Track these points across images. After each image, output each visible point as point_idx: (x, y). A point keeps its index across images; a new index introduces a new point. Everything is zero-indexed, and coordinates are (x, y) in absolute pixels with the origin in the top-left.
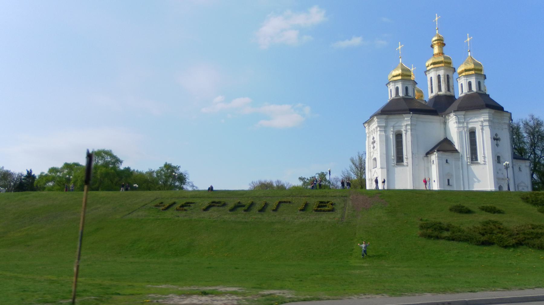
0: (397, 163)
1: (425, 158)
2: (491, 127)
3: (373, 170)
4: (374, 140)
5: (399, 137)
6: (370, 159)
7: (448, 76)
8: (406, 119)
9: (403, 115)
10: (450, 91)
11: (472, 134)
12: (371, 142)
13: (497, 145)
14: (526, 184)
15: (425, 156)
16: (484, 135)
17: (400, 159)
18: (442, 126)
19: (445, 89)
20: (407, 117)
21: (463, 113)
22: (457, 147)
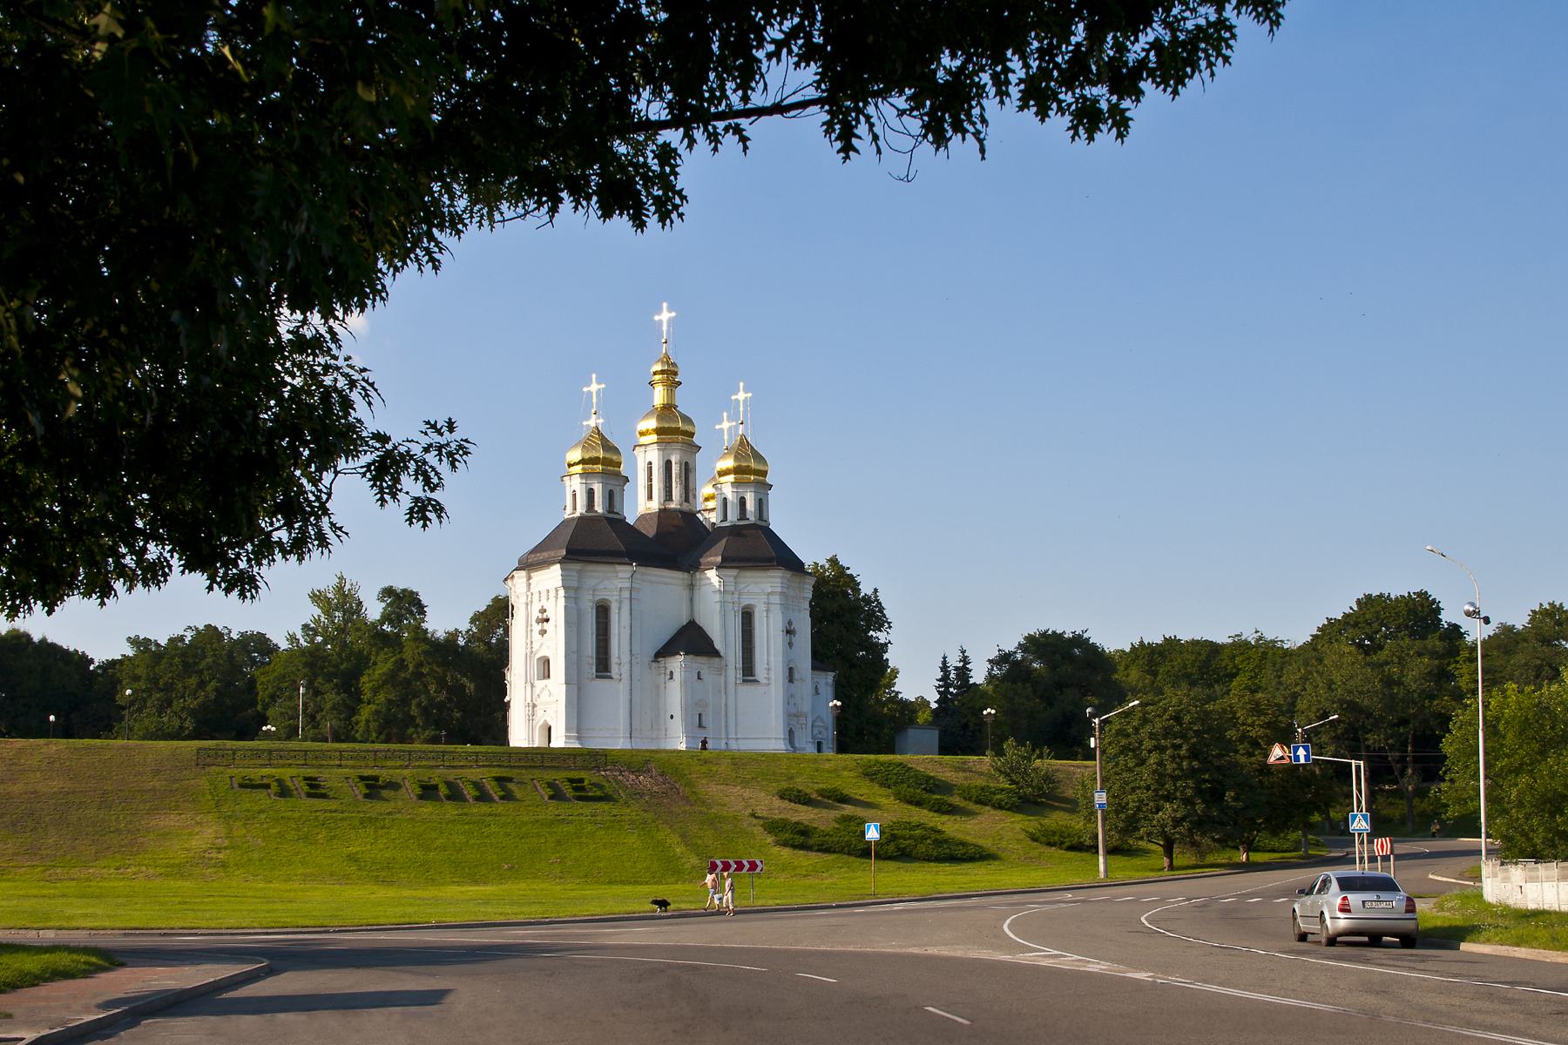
0: (598, 674)
1: (654, 665)
2: (785, 607)
3: (540, 684)
4: (545, 614)
5: (603, 611)
6: (530, 657)
7: (686, 463)
8: (620, 575)
9: (617, 566)
10: (689, 502)
11: (747, 617)
12: (534, 618)
13: (790, 644)
14: (824, 723)
15: (653, 659)
16: (771, 621)
17: (603, 665)
18: (685, 593)
19: (681, 497)
20: (625, 571)
21: (734, 572)
22: (718, 645)
